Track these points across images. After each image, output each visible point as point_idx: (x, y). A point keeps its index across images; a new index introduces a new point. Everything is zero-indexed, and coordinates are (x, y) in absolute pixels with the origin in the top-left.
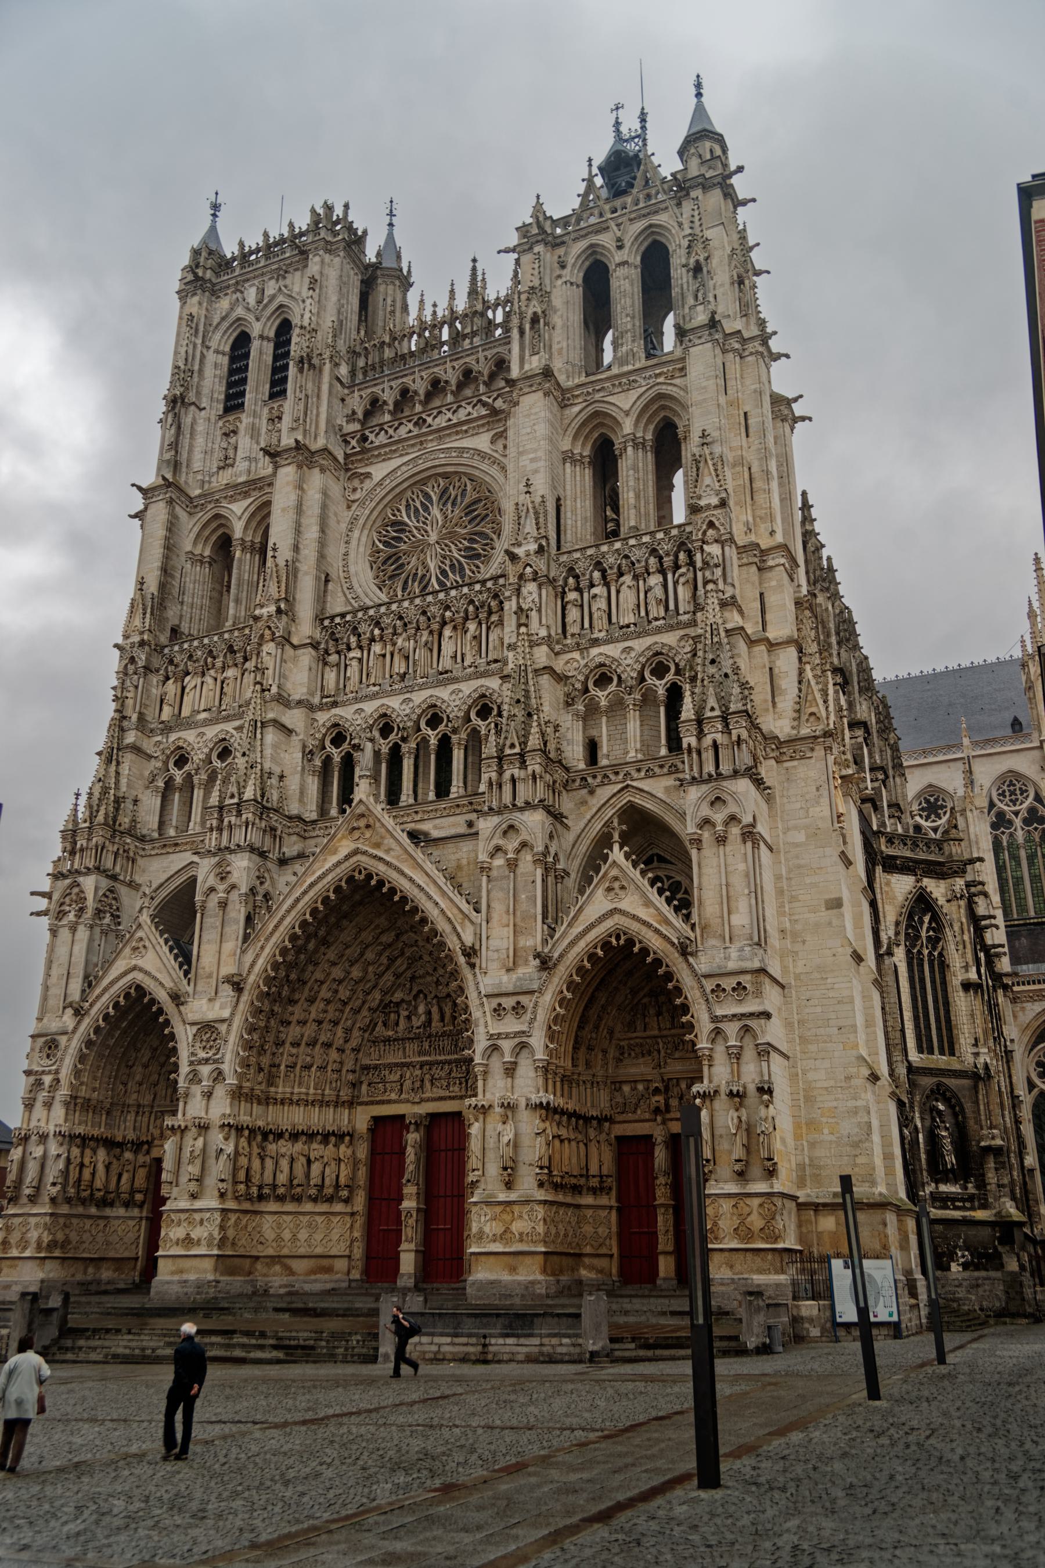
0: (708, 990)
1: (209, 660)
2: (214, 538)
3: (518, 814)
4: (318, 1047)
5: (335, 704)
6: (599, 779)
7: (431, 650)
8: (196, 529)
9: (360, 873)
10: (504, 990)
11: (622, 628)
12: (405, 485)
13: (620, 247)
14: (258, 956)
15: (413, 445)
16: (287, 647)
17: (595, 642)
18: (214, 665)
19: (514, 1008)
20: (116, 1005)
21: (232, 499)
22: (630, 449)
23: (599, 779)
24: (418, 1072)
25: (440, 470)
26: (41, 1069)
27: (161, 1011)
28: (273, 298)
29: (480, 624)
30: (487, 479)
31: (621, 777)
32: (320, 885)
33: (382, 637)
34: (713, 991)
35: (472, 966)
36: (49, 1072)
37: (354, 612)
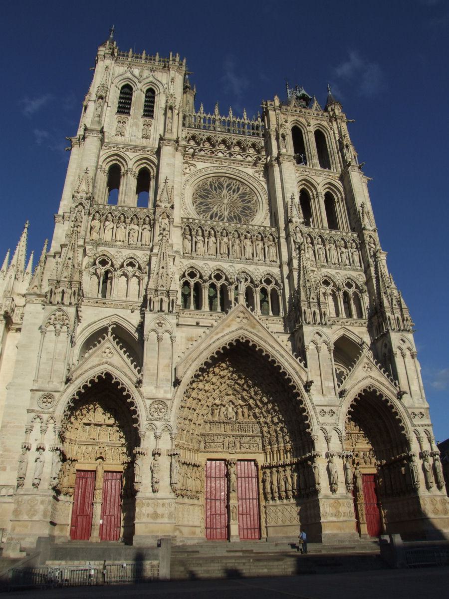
2: (111, 164)
3: (321, 328)
4: (187, 420)
5: (192, 258)
8: (105, 157)
9: (243, 339)
13: (310, 126)
14: (188, 369)
15: (216, 161)
17: (324, 266)
18: (125, 222)
19: (329, 412)
20: (92, 381)
24: (232, 439)
26: (41, 410)
27: (123, 389)
28: (147, 78)
29: (264, 244)
30: (251, 186)
31: (340, 323)
32: (221, 340)
35: (308, 391)
36: (48, 413)
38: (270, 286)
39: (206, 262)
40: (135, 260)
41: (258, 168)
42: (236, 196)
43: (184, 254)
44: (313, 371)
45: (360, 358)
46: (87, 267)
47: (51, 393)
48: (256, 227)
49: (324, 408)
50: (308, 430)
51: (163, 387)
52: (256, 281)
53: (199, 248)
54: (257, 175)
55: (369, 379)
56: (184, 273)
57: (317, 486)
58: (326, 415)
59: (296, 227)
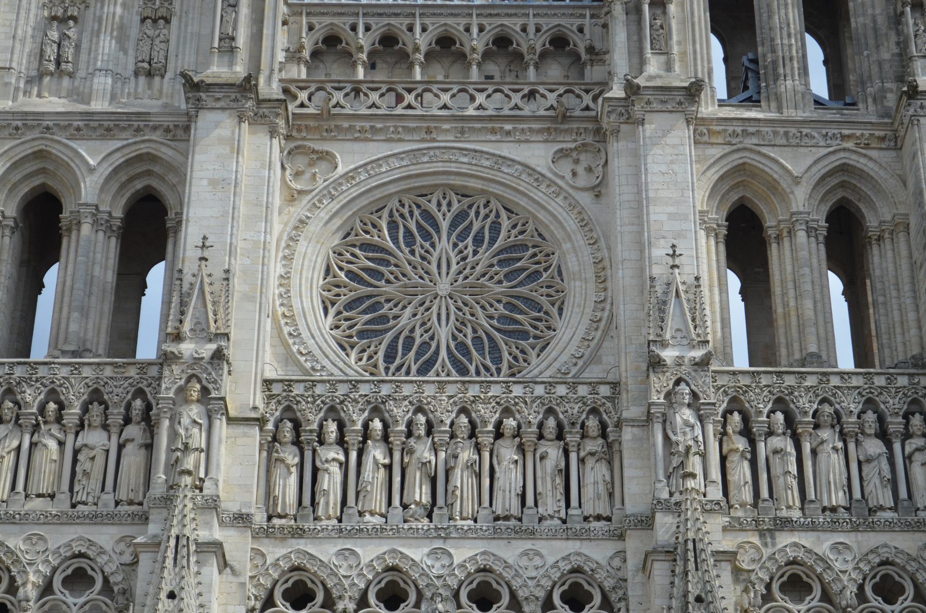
1: (52, 406)
2: (25, 189)
5: (298, 533)
7: (479, 476)
11: (824, 509)
12: (392, 189)
16: (224, 418)
17: (785, 524)
18: (59, 419)
21: (78, 133)
22: (801, 236)
25: (458, 181)
29: (566, 453)
30: (541, 215)
33: (386, 438)
37: (333, 384)
41: (568, 138)
42: (485, 256)
43: (270, 518)
48: (539, 390)
53: (326, 493)
54: (565, 168)
59: (678, 382)
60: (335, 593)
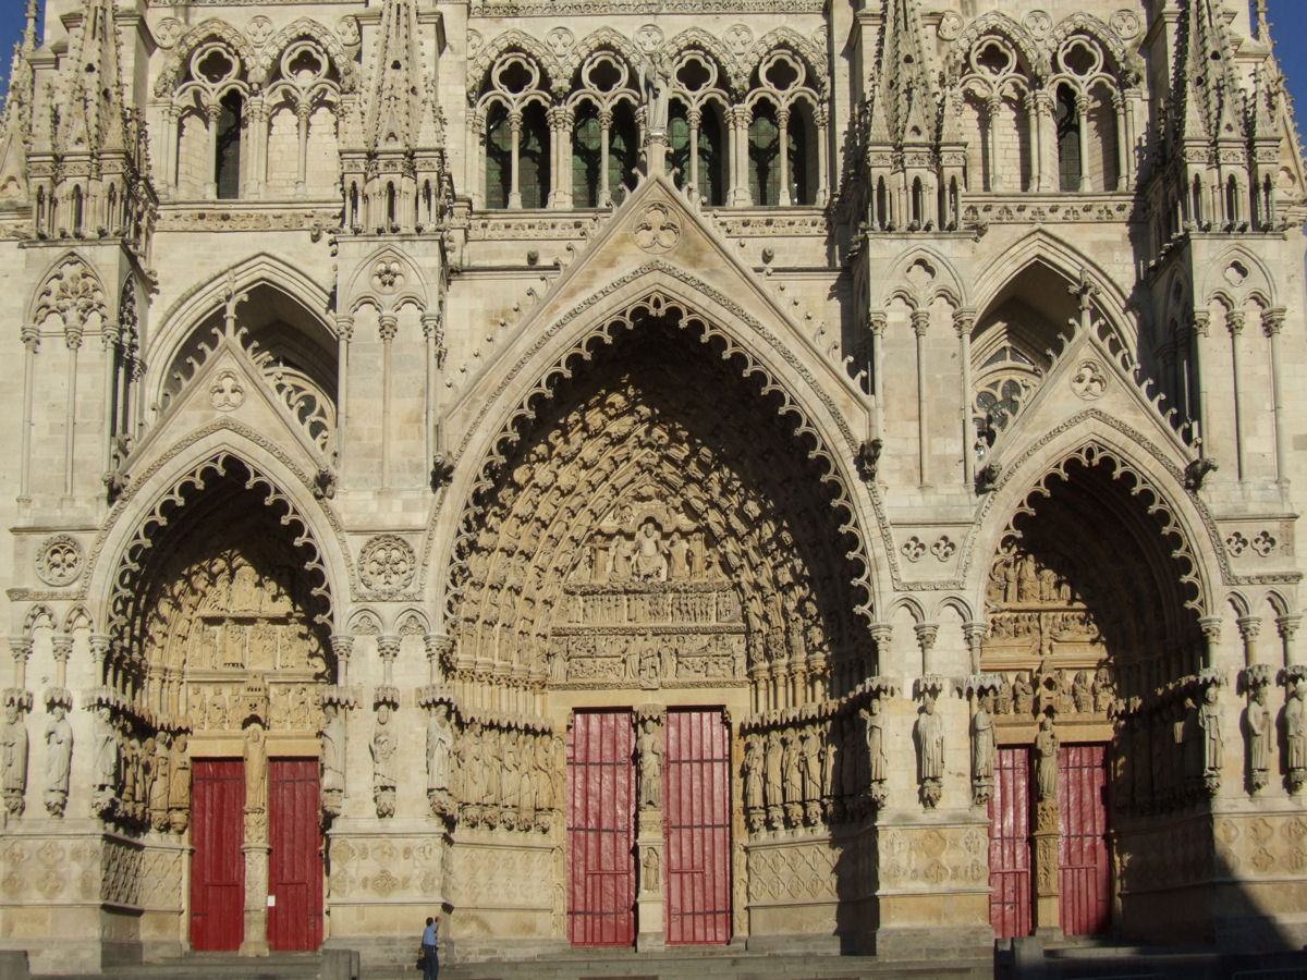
0: (1224, 538)
6: (995, 212)
10: (918, 518)
20: (187, 489)
23: (995, 212)
26: (46, 589)
27: (281, 507)
31: (1027, 214)
34: (1229, 541)
35: (867, 477)
36: (67, 597)
38: (789, 91)
39: (562, 22)
40: (318, 42)
44: (895, 406)
45: (1067, 346)
46: (160, 90)
47: (70, 534)
49: (920, 532)
50: (859, 609)
51: (400, 491)
52: (736, 76)
55: (1091, 421)
56: (488, 73)
57: (874, 786)
58: (927, 558)
60: (551, 71)
